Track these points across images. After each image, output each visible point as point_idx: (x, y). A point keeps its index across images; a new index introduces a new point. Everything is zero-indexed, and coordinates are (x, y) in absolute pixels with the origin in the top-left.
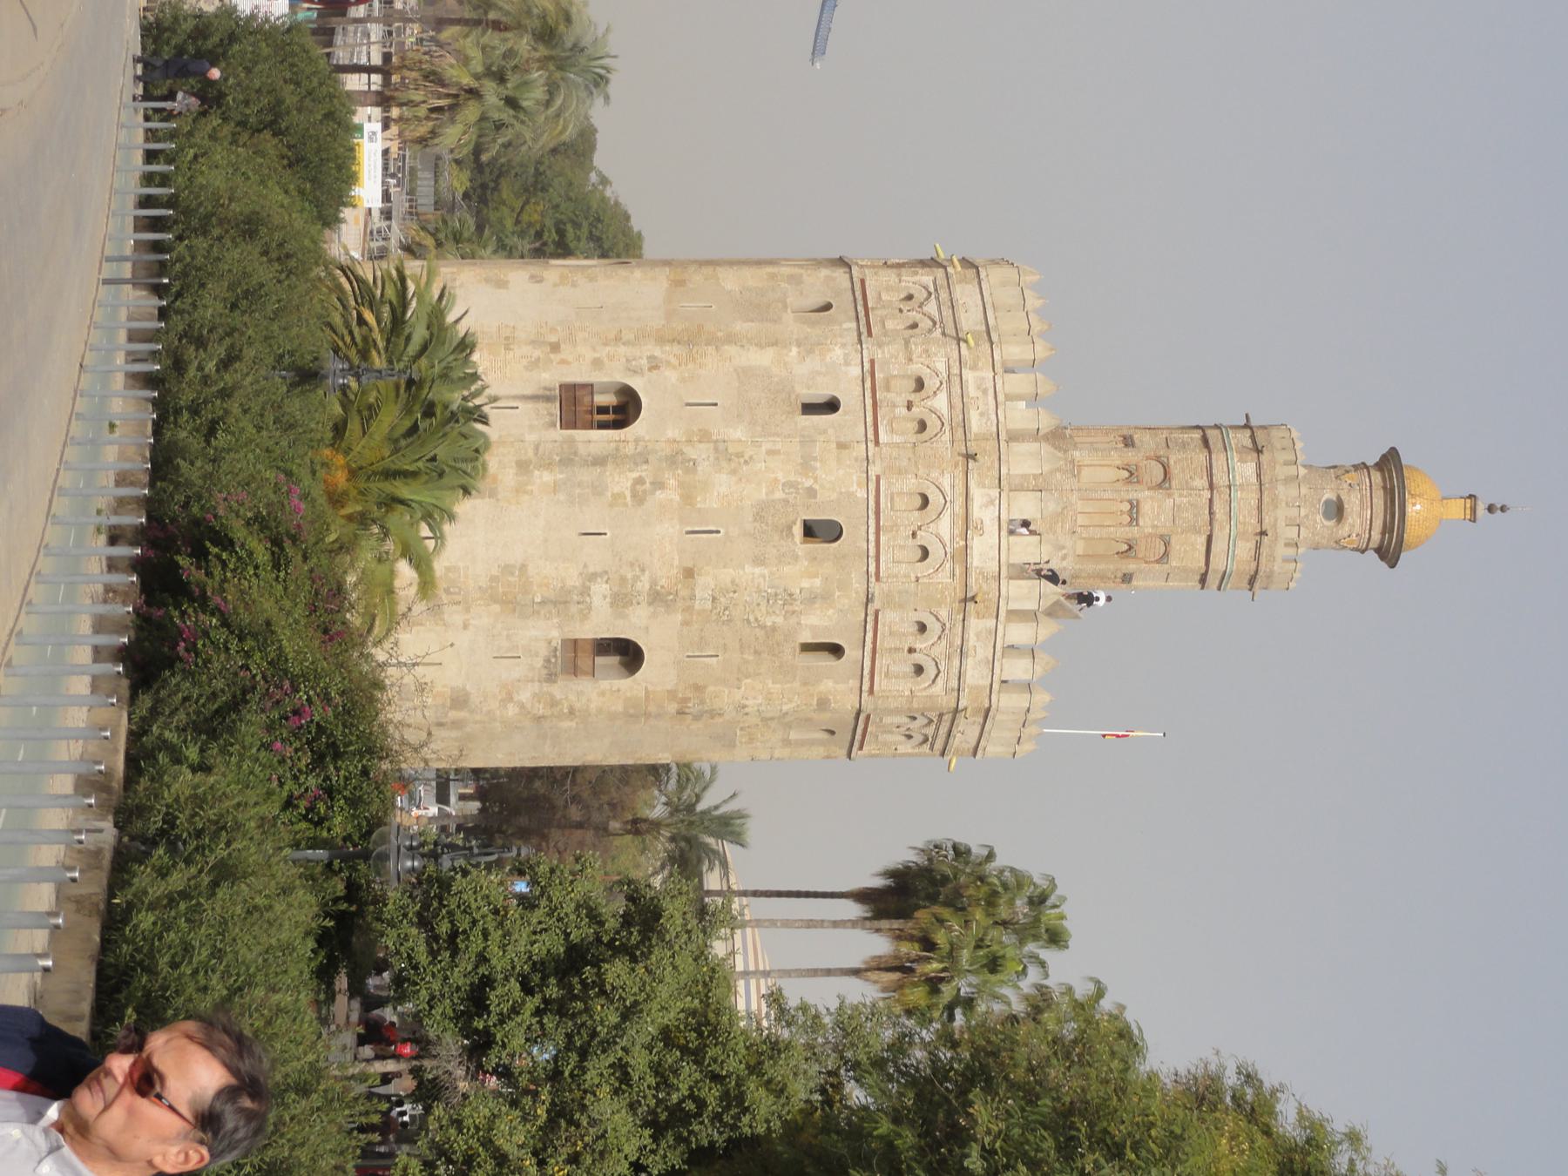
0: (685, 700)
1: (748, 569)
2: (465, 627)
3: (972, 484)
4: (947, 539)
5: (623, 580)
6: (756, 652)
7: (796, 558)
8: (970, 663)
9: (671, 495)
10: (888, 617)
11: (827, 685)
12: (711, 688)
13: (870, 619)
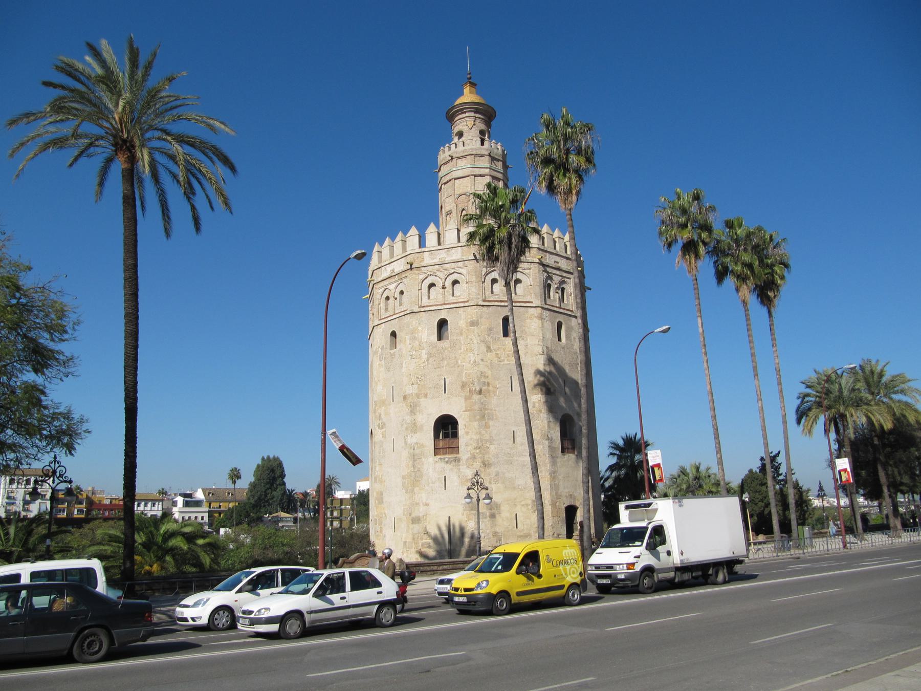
0: (471, 391)
1: (403, 370)
2: (427, 505)
3: (380, 279)
4: (395, 285)
5: (407, 429)
6: (443, 359)
7: (401, 349)
8: (448, 259)
9: (382, 410)
10: (425, 301)
11: (462, 323)
12: (464, 380)
13: (423, 309)
